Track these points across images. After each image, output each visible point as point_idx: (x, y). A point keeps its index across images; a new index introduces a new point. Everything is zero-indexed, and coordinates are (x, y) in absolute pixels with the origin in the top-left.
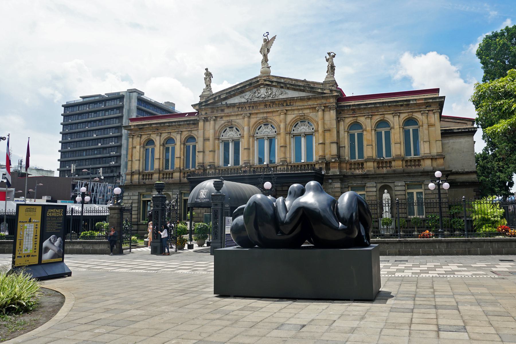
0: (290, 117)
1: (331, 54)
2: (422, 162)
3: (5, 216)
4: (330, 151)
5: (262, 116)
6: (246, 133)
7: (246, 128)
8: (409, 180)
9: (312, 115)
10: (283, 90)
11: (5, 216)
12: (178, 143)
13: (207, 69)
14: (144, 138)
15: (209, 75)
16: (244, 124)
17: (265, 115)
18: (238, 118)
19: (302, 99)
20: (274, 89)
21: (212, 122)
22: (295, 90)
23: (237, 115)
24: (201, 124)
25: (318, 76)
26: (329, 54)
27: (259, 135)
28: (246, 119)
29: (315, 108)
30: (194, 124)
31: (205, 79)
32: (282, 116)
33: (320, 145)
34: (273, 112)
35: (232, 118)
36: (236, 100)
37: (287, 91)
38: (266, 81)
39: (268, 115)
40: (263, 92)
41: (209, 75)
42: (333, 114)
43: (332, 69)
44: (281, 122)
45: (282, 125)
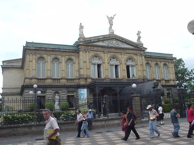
0: (126, 56)
1: (140, 32)
2: (170, 81)
3: (119, 111)
4: (143, 74)
5: (113, 54)
6: (106, 62)
7: (106, 59)
8: (168, 88)
9: (135, 57)
10: (122, 43)
11: (119, 111)
12: (63, 62)
13: (81, 24)
14: (38, 56)
15: (81, 27)
16: (106, 57)
17: (114, 54)
18: (101, 53)
19: (131, 49)
20: (119, 42)
21: (87, 53)
22: (128, 44)
23: (100, 51)
24: (81, 53)
25: (134, 39)
26: (139, 32)
27: (111, 63)
28: (106, 54)
29: (136, 54)
30: (76, 52)
31: (80, 29)
32: (123, 56)
33: (140, 72)
34: (117, 53)
35: (97, 52)
36: (101, 44)
37: (125, 44)
38: (112, 37)
39: (116, 54)
40: (114, 42)
41: (81, 27)
42: (143, 57)
43: (139, 38)
44: (122, 58)
45: (123, 60)
